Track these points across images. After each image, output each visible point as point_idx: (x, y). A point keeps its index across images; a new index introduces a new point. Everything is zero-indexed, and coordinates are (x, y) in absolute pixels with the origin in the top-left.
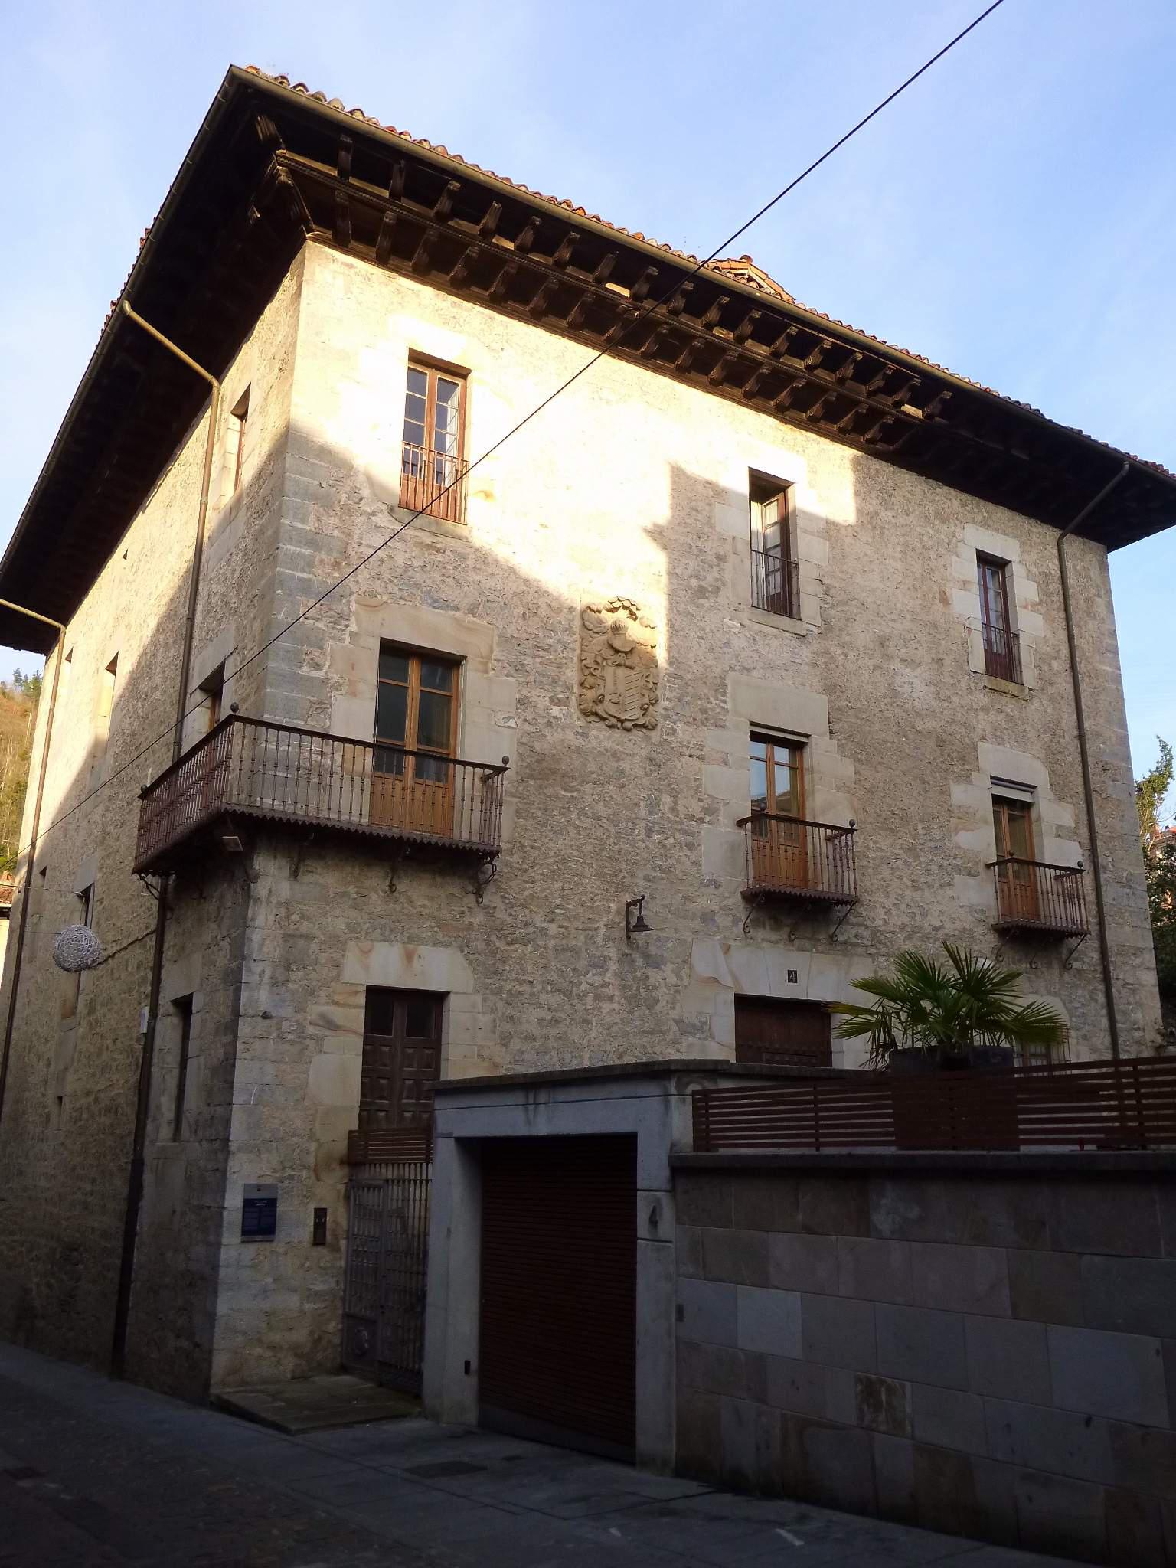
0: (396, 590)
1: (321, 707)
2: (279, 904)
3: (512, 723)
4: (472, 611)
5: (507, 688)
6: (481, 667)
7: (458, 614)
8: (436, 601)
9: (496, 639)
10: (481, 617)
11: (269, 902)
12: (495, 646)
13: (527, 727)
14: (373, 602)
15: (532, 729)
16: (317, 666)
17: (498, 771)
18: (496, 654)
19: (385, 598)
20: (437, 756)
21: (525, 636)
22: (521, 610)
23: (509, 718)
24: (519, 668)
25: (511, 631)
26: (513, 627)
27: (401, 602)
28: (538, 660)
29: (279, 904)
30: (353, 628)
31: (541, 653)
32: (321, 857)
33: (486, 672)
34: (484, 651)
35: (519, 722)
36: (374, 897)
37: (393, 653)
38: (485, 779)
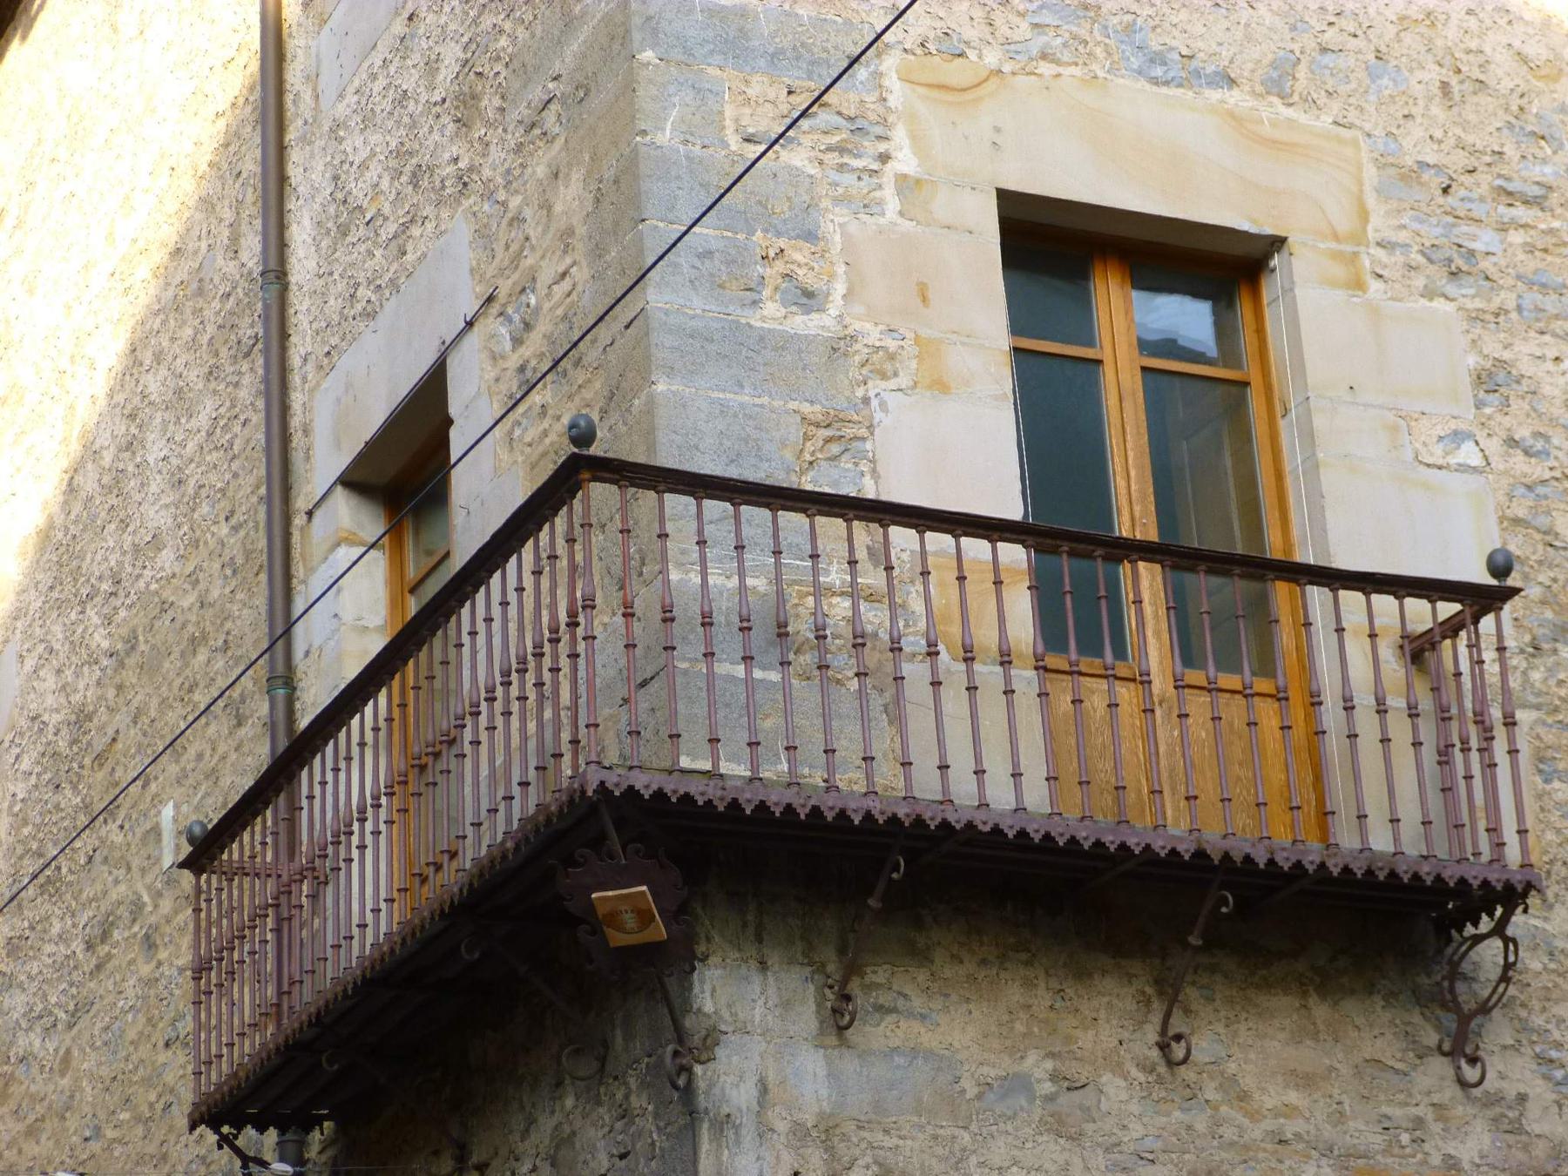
0: (1023, 30)
1: (840, 430)
2: (800, 1133)
3: (1468, 454)
4: (1278, 83)
5: (1432, 341)
6: (1339, 271)
7: (1235, 98)
8: (1158, 59)
9: (1370, 173)
10: (1310, 102)
11: (764, 1131)
12: (1371, 201)
13: (1519, 461)
14: (955, 72)
15: (1538, 470)
16: (808, 299)
17: (1482, 599)
18: (1379, 224)
19: (992, 58)
20: (1240, 574)
21: (1460, 160)
22: (1433, 74)
23: (1458, 437)
24: (1458, 267)
25: (1414, 146)
26: (1417, 131)
27: (1046, 68)
28: (1517, 237)
29: (800, 1133)
30: (905, 161)
31: (1521, 213)
32: (920, 956)
33: (1358, 285)
34: (1344, 222)
35: (1494, 446)
36: (1114, 1087)
37: (1051, 245)
38: (1418, 650)
